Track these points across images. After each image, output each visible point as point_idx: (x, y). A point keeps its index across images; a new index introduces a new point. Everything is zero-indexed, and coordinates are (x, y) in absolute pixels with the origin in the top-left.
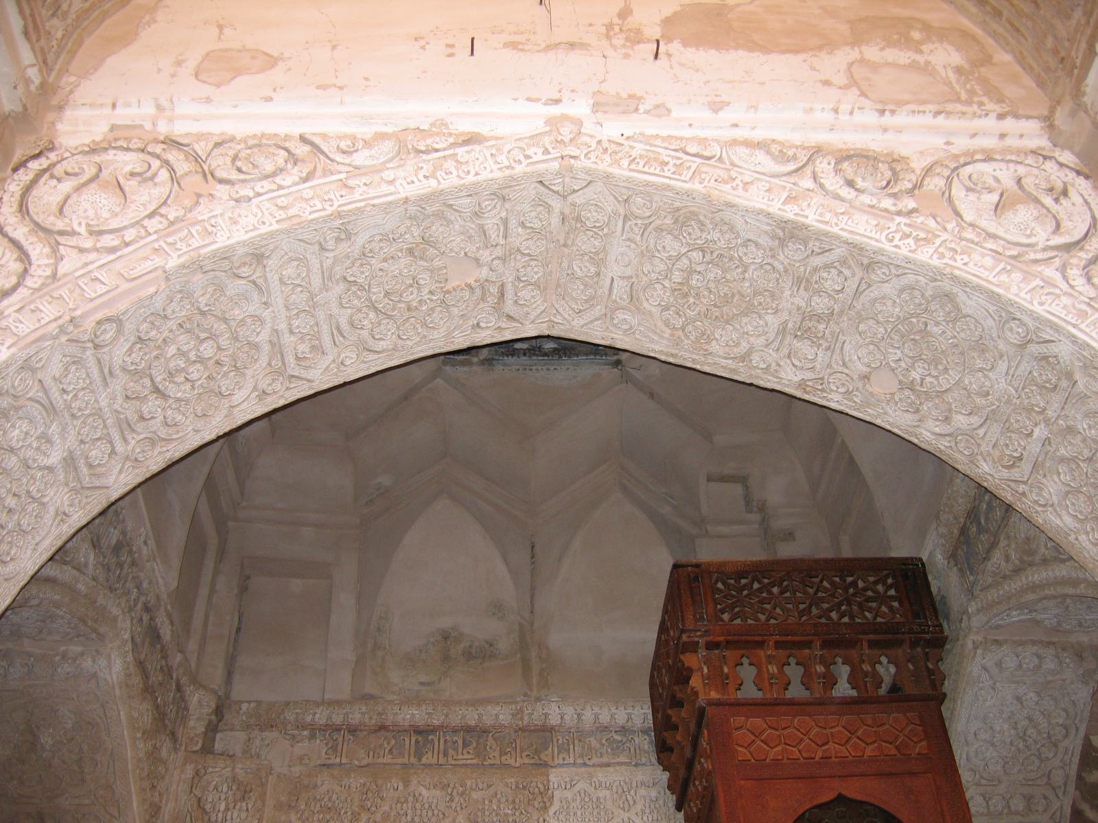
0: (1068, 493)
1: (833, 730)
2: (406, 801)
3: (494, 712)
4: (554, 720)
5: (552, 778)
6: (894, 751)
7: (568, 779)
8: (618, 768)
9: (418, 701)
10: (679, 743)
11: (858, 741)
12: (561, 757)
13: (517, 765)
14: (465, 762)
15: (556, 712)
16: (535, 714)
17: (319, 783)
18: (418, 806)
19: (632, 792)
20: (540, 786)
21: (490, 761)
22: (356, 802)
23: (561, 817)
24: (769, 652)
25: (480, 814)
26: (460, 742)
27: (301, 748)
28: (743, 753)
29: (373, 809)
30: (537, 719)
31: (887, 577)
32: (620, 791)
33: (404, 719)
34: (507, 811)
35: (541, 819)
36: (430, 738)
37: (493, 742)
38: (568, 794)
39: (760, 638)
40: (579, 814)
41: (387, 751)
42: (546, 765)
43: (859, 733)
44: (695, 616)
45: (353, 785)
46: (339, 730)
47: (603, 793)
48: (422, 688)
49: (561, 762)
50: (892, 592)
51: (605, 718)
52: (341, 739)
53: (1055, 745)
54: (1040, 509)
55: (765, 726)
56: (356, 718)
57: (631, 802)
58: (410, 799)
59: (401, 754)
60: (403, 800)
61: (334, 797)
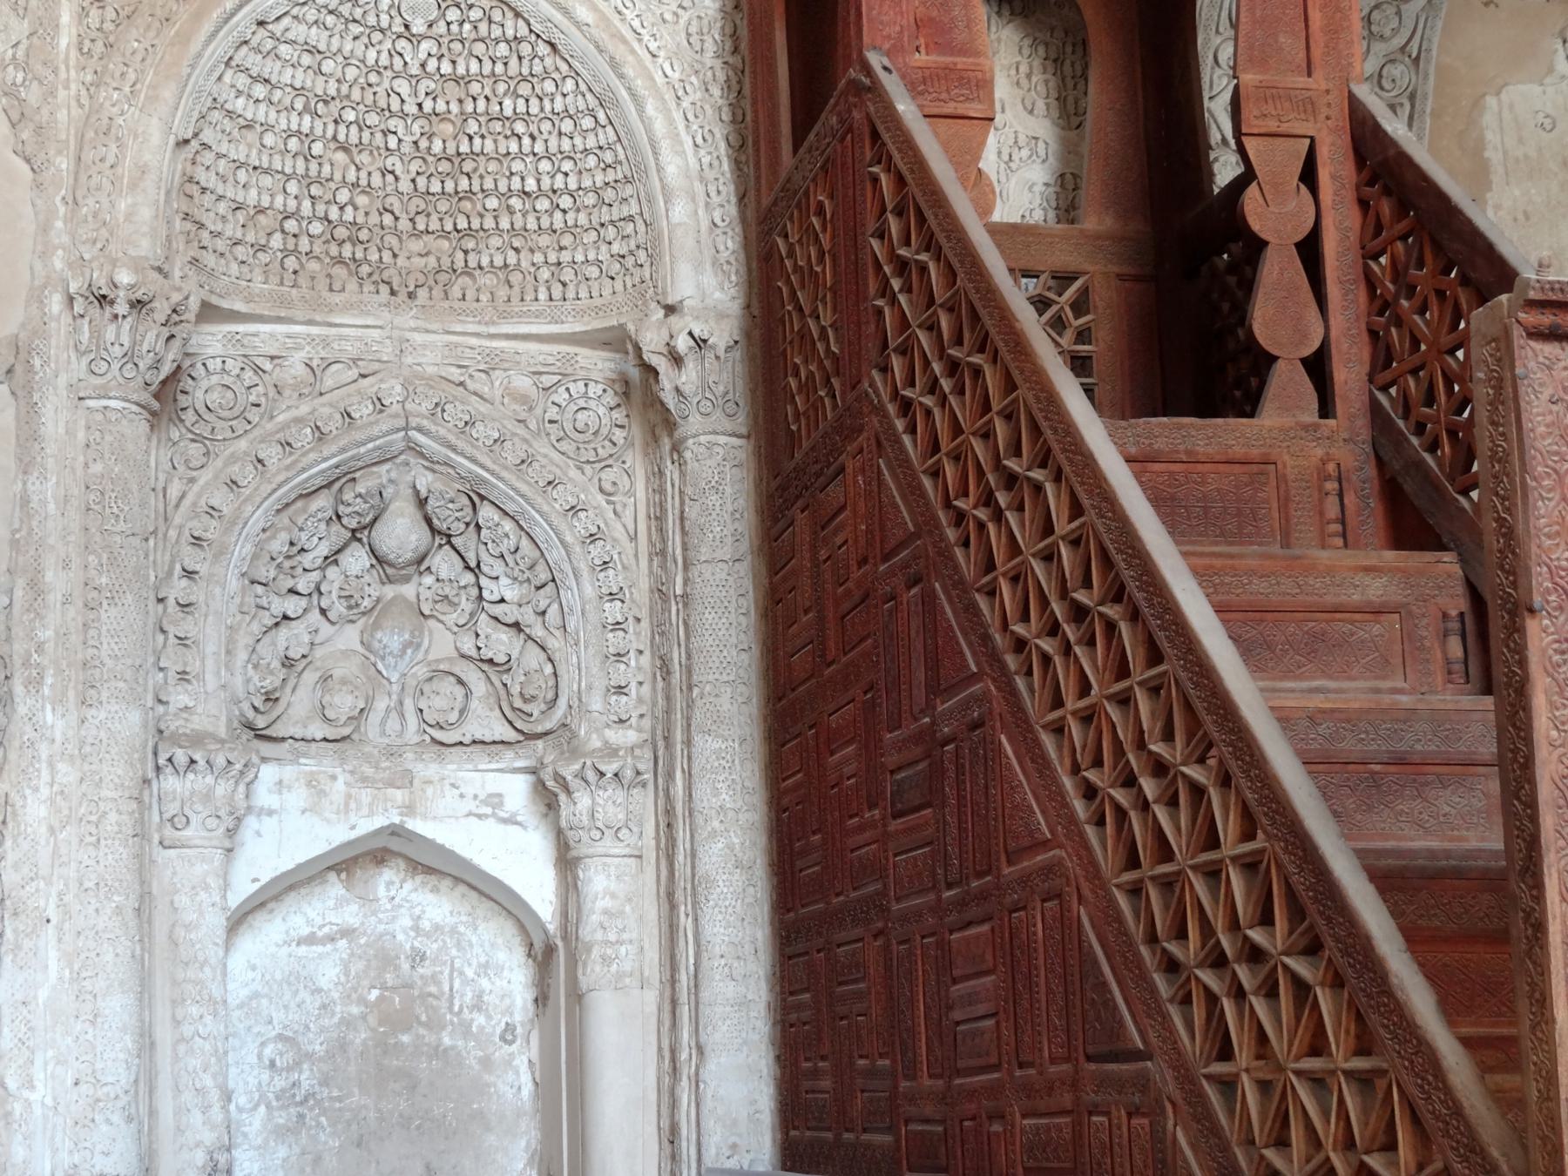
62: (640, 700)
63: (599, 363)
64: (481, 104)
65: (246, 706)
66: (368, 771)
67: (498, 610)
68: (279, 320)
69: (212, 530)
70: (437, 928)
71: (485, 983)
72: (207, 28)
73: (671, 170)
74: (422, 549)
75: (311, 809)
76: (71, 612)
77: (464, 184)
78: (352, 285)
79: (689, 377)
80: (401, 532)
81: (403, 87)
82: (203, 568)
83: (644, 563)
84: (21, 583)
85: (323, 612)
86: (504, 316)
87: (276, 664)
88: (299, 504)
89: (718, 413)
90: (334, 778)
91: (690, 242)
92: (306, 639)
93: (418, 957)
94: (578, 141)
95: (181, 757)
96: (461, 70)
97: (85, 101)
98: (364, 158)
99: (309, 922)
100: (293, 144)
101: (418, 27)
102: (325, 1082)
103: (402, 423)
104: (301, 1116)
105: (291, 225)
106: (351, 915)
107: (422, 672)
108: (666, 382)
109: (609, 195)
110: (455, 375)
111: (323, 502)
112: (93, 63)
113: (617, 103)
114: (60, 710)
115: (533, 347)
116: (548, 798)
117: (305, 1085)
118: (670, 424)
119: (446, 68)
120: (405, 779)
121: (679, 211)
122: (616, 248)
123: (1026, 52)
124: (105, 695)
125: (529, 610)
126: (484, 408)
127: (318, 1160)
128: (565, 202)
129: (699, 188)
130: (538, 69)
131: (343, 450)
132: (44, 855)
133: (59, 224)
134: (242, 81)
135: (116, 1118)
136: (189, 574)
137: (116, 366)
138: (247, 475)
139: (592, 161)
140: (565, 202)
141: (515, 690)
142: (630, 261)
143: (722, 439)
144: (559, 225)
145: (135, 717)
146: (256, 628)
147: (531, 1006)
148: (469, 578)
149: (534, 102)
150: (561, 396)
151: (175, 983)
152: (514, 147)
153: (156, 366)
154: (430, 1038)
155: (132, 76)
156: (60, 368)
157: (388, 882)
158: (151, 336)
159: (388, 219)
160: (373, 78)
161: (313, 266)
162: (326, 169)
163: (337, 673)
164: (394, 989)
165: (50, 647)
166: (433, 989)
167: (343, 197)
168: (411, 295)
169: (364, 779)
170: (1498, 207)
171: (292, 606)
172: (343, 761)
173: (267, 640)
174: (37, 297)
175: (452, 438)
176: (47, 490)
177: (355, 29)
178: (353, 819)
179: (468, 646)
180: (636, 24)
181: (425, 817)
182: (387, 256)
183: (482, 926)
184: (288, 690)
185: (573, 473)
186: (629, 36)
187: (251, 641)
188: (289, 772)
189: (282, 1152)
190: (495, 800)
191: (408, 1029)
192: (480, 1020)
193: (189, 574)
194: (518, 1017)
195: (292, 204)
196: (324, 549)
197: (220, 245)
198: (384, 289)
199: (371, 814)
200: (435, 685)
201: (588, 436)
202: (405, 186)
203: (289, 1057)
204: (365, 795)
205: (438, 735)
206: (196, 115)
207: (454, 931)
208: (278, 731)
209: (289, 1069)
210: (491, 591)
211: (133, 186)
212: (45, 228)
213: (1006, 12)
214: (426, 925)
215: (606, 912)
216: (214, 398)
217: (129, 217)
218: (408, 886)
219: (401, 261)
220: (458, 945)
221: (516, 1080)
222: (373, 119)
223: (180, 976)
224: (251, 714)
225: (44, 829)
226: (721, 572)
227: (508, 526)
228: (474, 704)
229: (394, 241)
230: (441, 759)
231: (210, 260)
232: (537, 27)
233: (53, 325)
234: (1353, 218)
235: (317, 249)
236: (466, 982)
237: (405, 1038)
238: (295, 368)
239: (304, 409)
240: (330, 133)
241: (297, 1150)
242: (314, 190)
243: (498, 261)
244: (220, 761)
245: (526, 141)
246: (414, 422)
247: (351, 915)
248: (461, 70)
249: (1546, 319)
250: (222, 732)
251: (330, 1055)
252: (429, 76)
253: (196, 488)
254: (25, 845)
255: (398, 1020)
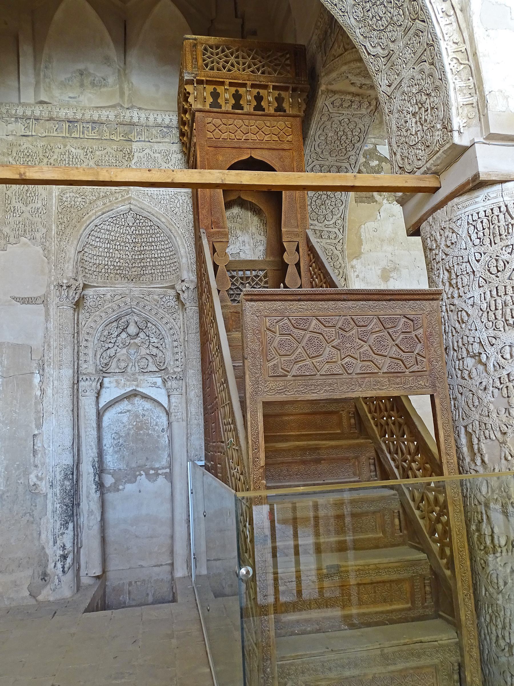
0: (354, 5)
1: (251, 127)
2: (65, 154)
3: (107, 114)
4: (135, 120)
5: (133, 147)
6: (277, 139)
7: (141, 148)
8: (164, 144)
9: (68, 106)
10: (186, 130)
11: (262, 133)
12: (138, 137)
13: (118, 140)
14: (92, 137)
15: (135, 115)
16: (127, 115)
17: (22, 144)
18: (71, 157)
19: (170, 156)
20: (128, 150)
21: (105, 138)
22: (41, 154)
23: (137, 165)
24: (226, 87)
25: (100, 161)
26: (90, 128)
27: (10, 127)
28: (209, 135)
29: (49, 157)
30: (127, 120)
31: (287, 54)
32: (165, 154)
33: (62, 115)
34: (112, 161)
35: (128, 166)
36: (75, 125)
37: (106, 129)
38: (141, 155)
39: (222, 80)
40: (146, 164)
41: (55, 130)
42: (131, 141)
43: (263, 130)
44: (192, 66)
45: (39, 146)
46: (30, 119)
47: (157, 155)
48: (70, 99)
49: (138, 140)
50: (288, 62)
51: (159, 120)
52: (31, 123)
53: (354, 145)
54: (341, 14)
55: (221, 123)
56: (37, 113)
57: (170, 160)
58: (67, 153)
59: (62, 132)
60: (63, 153)
61: (30, 151)
62: (181, 362)
63: (172, 292)
64: (145, 239)
65: (100, 366)
66: (129, 378)
67: (153, 344)
68: (104, 287)
69: (91, 331)
70: (148, 409)
71: (158, 420)
72: (83, 228)
73: (182, 252)
74: (137, 332)
75: (117, 387)
76: (57, 350)
77: (142, 256)
78: (120, 279)
79: (185, 295)
80: (132, 329)
81: (129, 237)
82: (89, 339)
83: (182, 333)
84: (46, 345)
85: (118, 346)
86: (151, 283)
87: (107, 358)
88: (110, 324)
89: (192, 302)
90: (121, 380)
91: (186, 266)
92: (114, 352)
93: (144, 415)
94: (165, 246)
95: (85, 379)
96: (140, 233)
97: (58, 245)
98: (122, 252)
99: (121, 409)
100: (106, 250)
101: (131, 224)
102: (125, 442)
103: (130, 307)
104: (120, 449)
105: (106, 267)
106: (129, 407)
107: (139, 357)
108: (181, 296)
109: (172, 257)
110: (142, 296)
111: (115, 324)
112: (60, 237)
113: (172, 238)
114: (54, 371)
115: (158, 289)
116: (164, 381)
117: (121, 442)
118: (183, 305)
119: (137, 232)
120: (136, 380)
121: (184, 260)
122: (174, 268)
123: (259, 222)
124: (64, 367)
125: (159, 344)
126: (148, 303)
127: (124, 457)
128: (163, 259)
129: (188, 255)
130: (156, 232)
131: (118, 313)
132: (51, 401)
133: (53, 271)
134: (93, 238)
135: (67, 453)
136: (86, 340)
137: (65, 299)
138: (98, 319)
139: (168, 250)
140: (163, 259)
141: (158, 361)
142: (176, 271)
143: (193, 308)
144: (162, 264)
145: (71, 371)
146: (102, 350)
147: (168, 425)
148: (147, 338)
149: (156, 238)
150: (164, 300)
151: (85, 424)
152: (152, 248)
153: (74, 298)
154: (147, 432)
155: (67, 239)
156: (54, 300)
157: (137, 400)
158: (72, 293)
159: (127, 265)
160: (122, 235)
161: (112, 275)
162: (113, 255)
163: (121, 359)
164: (139, 422)
165: (52, 358)
166: (147, 422)
167: (117, 260)
168: (132, 280)
169: (128, 380)
170: (364, 249)
171: (110, 345)
172: (123, 376)
173: (105, 352)
174: (49, 286)
175: (140, 310)
176: (51, 326)
177: (118, 226)
178: (125, 388)
179: (148, 352)
180: (175, 221)
181: (140, 387)
182: (127, 272)
183: (157, 408)
184: (111, 363)
185: (167, 315)
186: (173, 224)
187: (101, 353)
188: (112, 379)
189: (116, 456)
190: (155, 383)
191: (141, 430)
192: (157, 428)
193: (86, 340)
194: (165, 427)
195: (106, 263)
196: (116, 334)
197: (90, 272)
198: (126, 279)
199: (129, 387)
200: (142, 360)
201: (170, 307)
202: (130, 257)
203: (118, 437)
204: (128, 383)
205: (143, 370)
206: (82, 246)
207: (151, 410)
208: (108, 371)
209: (117, 439)
210: (152, 340)
211: (68, 262)
212: (50, 272)
213: (255, 214)
214: (145, 409)
215: (175, 406)
216: (91, 304)
217: (67, 268)
218: (141, 401)
219: (130, 273)
220: (152, 413)
221: (165, 440)
222: (123, 244)
223: (86, 422)
224: (101, 368)
225: (52, 395)
226: (193, 335)
227: (154, 327)
228: (150, 364)
229: (128, 269)
230: (144, 375)
231: (88, 275)
232: (155, 223)
233: (52, 291)
234: (307, 258)
235: (112, 272)
236: (154, 420)
237: (141, 432)
238: (108, 296)
239: (110, 305)
240: (114, 248)
241: (119, 455)
242: (111, 259)
243: (150, 272)
244: (93, 378)
245: (155, 247)
246: (132, 306)
247: (129, 407)
248: (140, 233)
249: (250, 297)
250: (94, 372)
251: (126, 436)
252: (134, 234)
253: (88, 322)
254: (48, 398)
255: (140, 428)
